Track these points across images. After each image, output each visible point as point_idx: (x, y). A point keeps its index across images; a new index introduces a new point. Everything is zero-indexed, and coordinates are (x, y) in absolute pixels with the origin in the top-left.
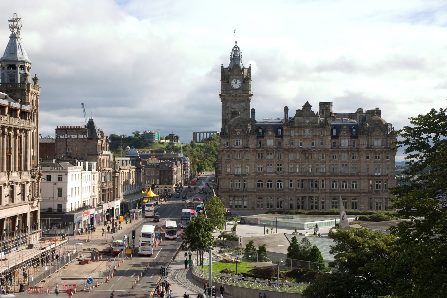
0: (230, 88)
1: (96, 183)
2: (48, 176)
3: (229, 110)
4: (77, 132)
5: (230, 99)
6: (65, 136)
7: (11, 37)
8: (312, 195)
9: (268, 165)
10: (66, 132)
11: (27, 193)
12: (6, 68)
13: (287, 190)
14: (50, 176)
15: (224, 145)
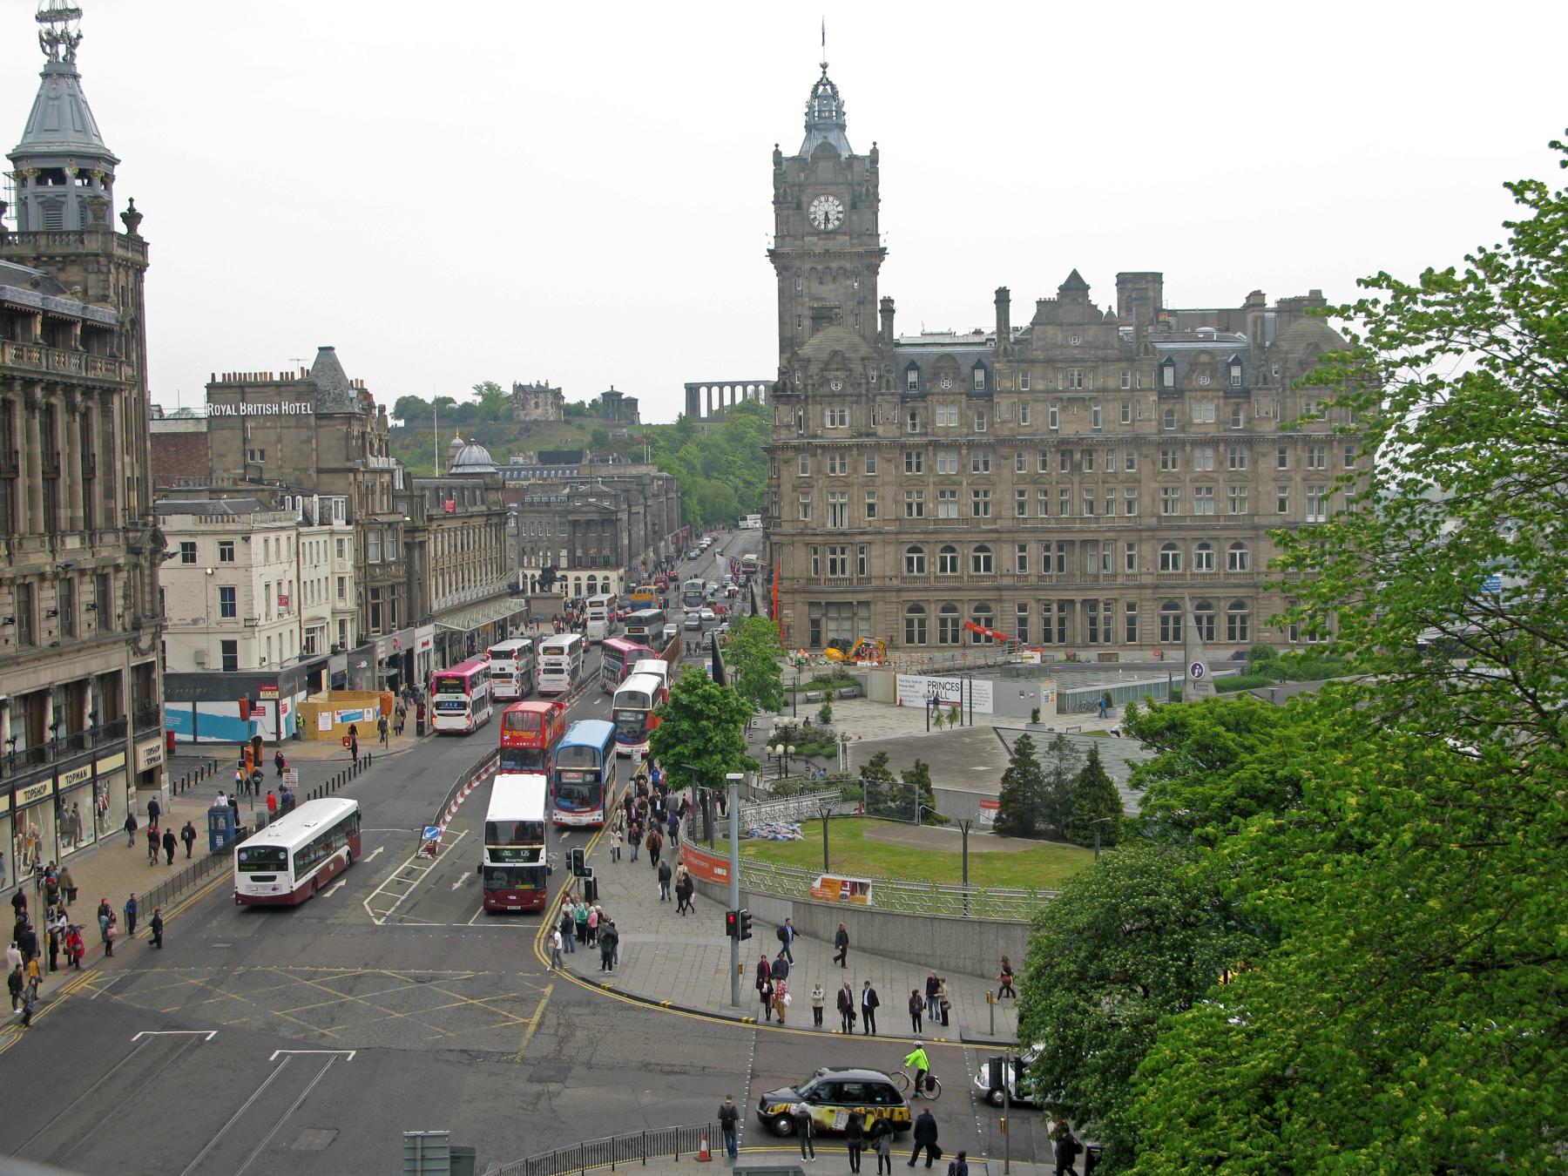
0: (807, 229)
1: (347, 565)
2: (184, 545)
3: (803, 304)
4: (279, 394)
5: (808, 266)
6: (237, 410)
7: (45, 75)
8: (1092, 595)
9: (943, 494)
10: (243, 393)
11: (118, 605)
12: (31, 181)
13: (1007, 581)
14: (193, 545)
15: (788, 426)
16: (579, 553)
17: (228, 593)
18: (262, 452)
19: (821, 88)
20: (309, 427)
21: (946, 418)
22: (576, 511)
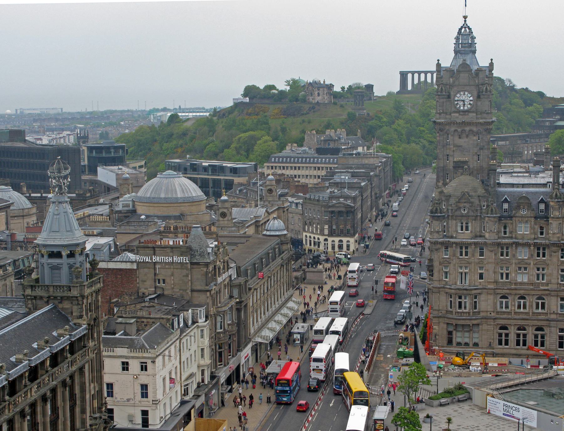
0: (453, 109)
2: (123, 363)
3: (450, 149)
4: (172, 252)
5: (453, 129)
6: (151, 259)
9: (520, 268)
10: (154, 251)
13: (553, 316)
14: (127, 363)
15: (438, 232)
16: (334, 227)
17: (144, 387)
18: (164, 281)
19: (463, 29)
20: (187, 269)
21: (524, 230)
22: (333, 206)
